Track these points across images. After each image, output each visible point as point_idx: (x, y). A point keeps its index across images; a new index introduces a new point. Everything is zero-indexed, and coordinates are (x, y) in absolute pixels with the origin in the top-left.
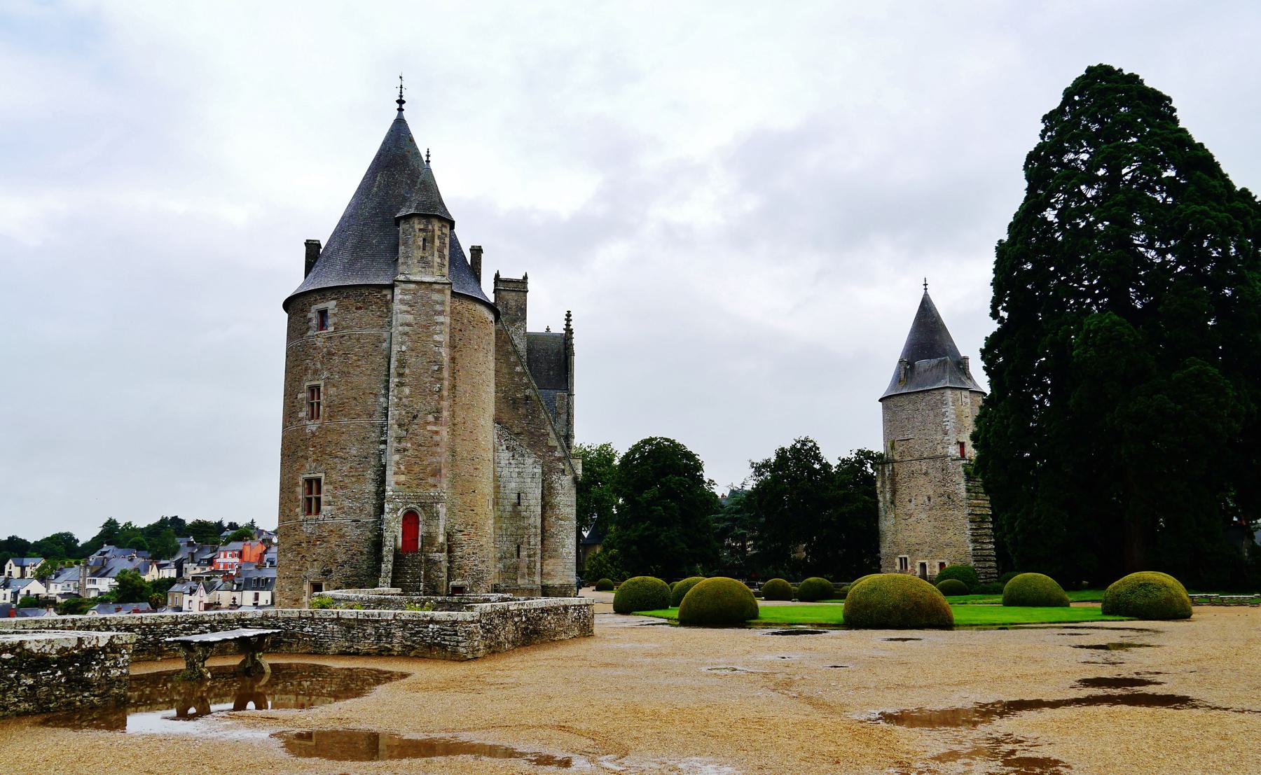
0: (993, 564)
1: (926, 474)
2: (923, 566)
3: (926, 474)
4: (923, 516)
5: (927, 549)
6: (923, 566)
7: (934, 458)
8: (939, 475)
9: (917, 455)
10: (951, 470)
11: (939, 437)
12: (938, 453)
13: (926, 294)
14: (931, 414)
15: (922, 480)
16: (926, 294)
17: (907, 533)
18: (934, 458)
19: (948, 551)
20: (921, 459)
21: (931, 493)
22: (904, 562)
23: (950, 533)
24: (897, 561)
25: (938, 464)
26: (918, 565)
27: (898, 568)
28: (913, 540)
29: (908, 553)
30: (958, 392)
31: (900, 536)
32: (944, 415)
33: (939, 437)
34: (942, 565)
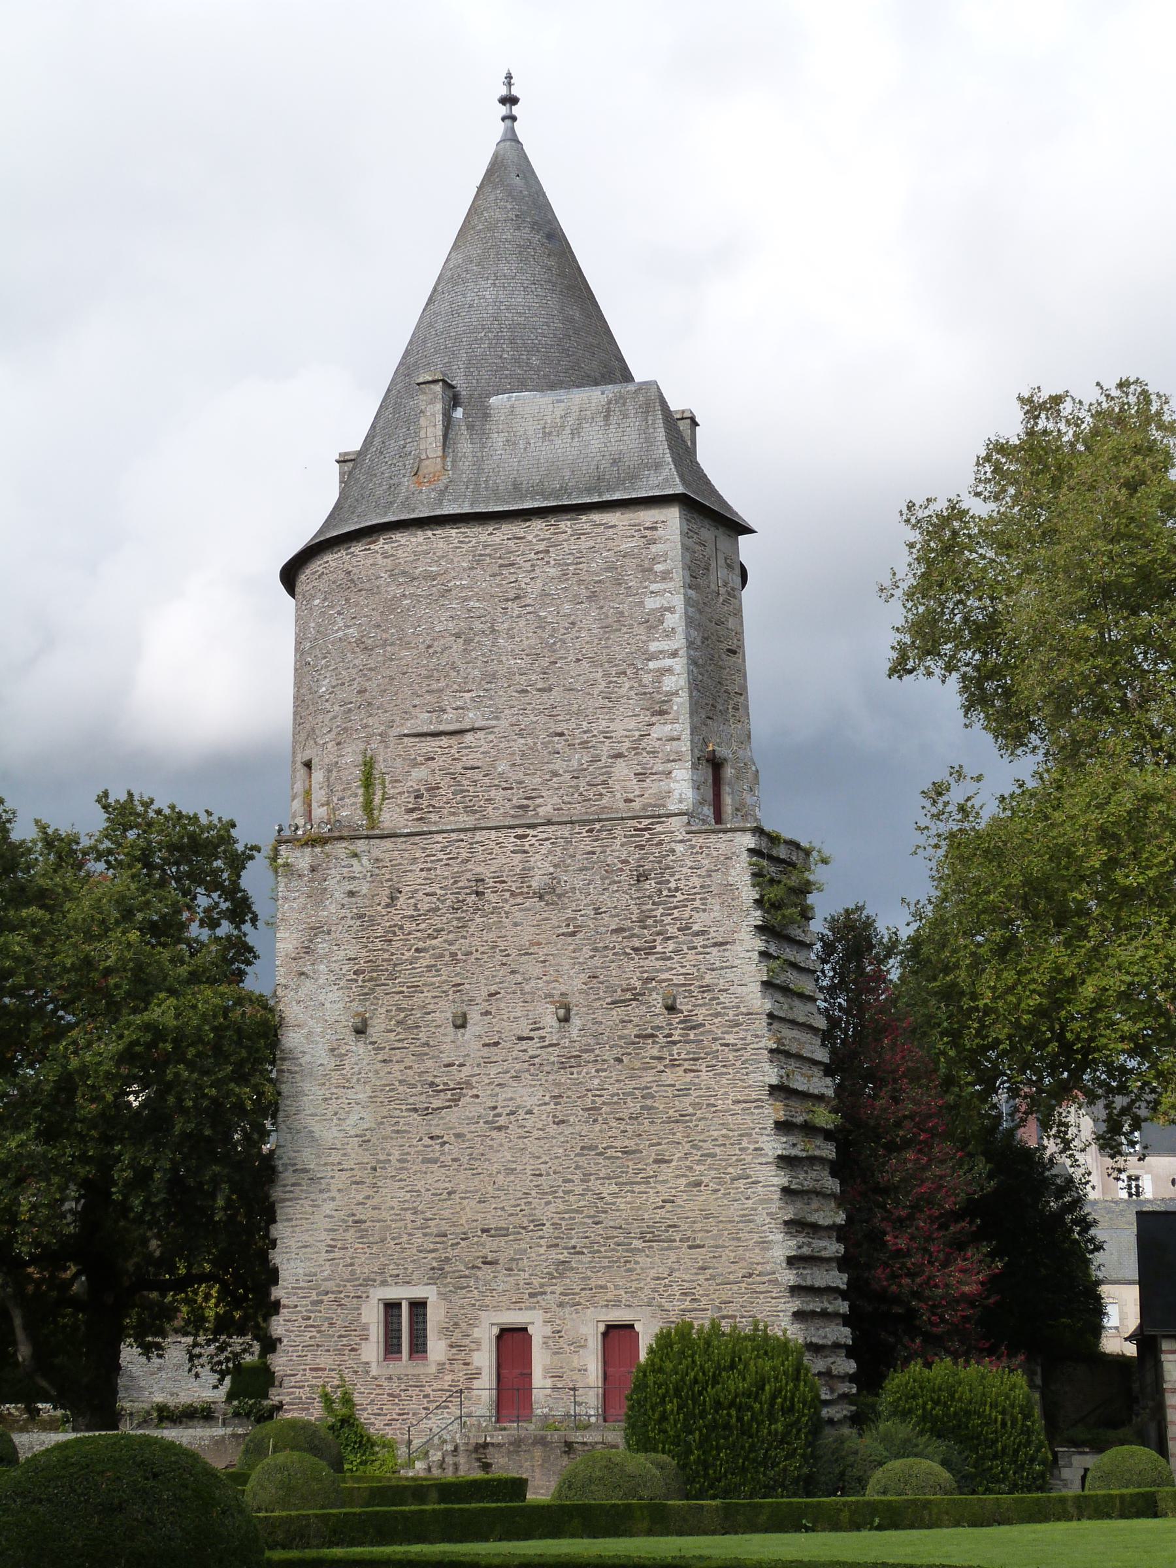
0: (844, 1334)
1: (548, 894)
2: (513, 1343)
3: (548, 894)
4: (527, 1094)
5: (541, 1256)
6: (513, 1343)
7: (594, 823)
8: (621, 900)
9: (500, 808)
10: (685, 876)
11: (625, 725)
12: (614, 802)
13: (511, 137)
14: (589, 618)
15: (524, 924)
16: (511, 137)
17: (436, 1178)
18: (594, 823)
19: (652, 1264)
20: (523, 823)
21: (573, 984)
22: (405, 1328)
23: (671, 1180)
24: (372, 1317)
25: (618, 849)
26: (485, 1334)
27: (372, 1350)
28: (470, 1213)
29: (437, 1274)
30: (707, 533)
31: (393, 1195)
32: (653, 622)
33: (625, 725)
34: (617, 1335)
